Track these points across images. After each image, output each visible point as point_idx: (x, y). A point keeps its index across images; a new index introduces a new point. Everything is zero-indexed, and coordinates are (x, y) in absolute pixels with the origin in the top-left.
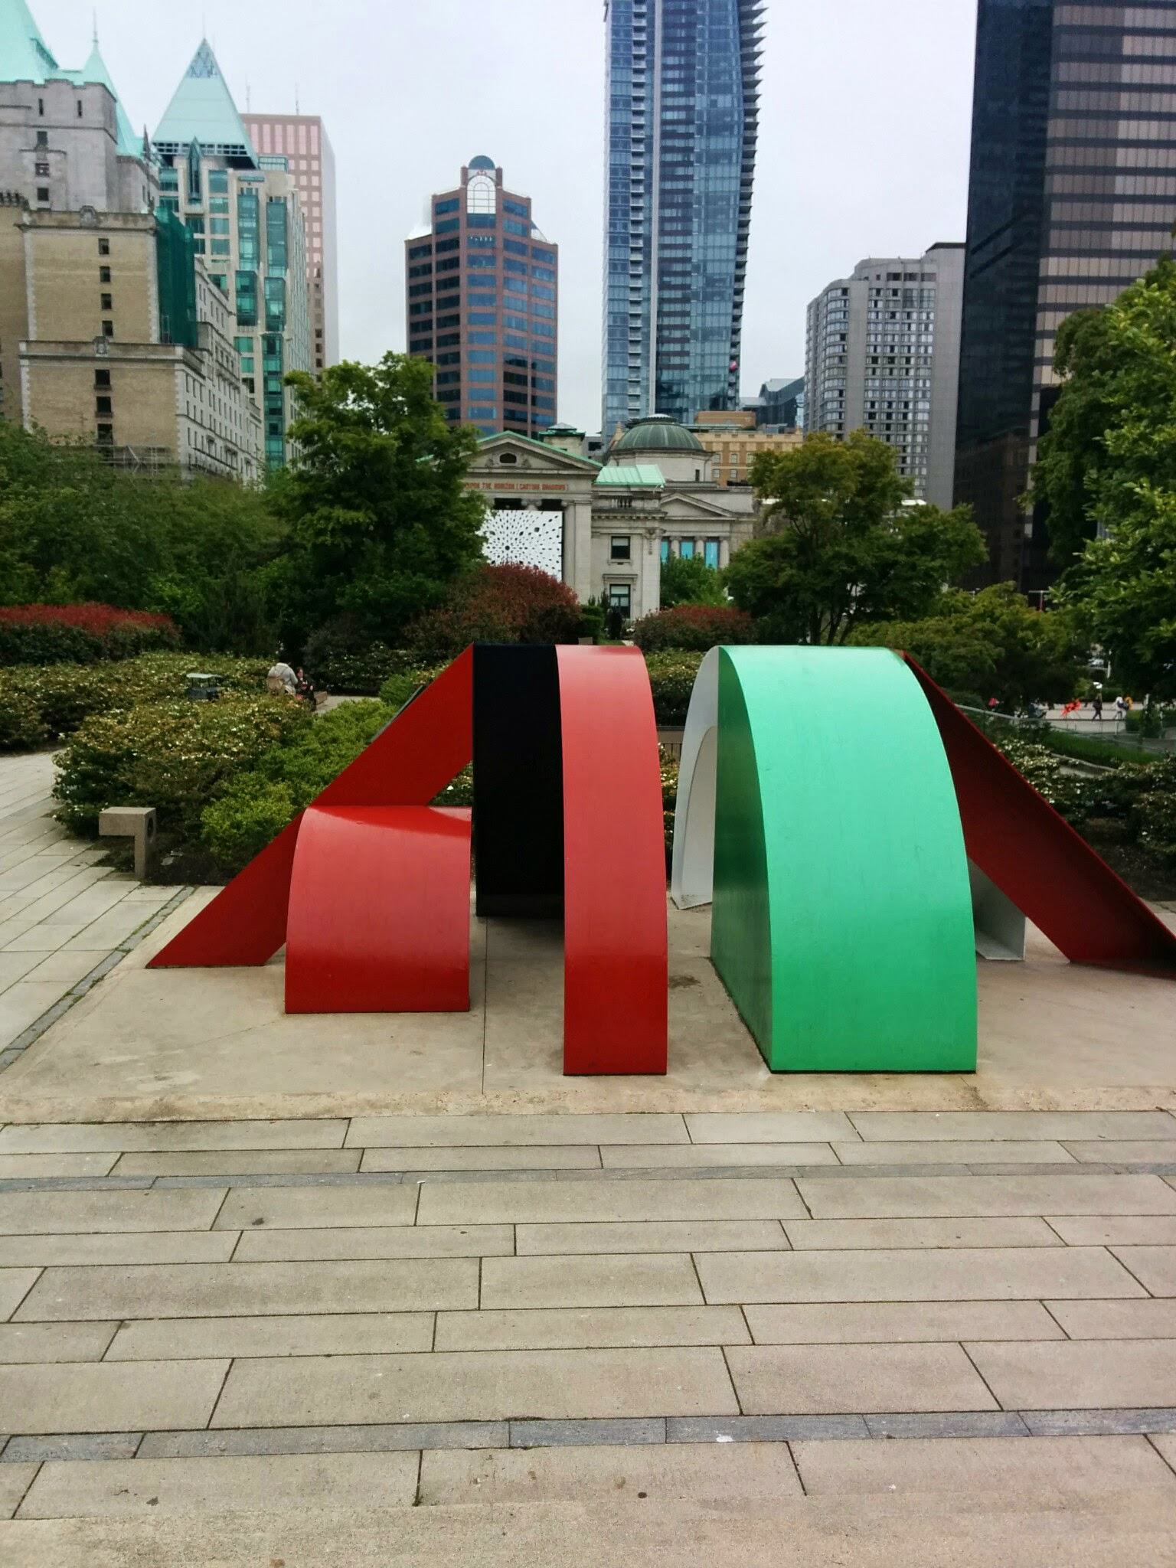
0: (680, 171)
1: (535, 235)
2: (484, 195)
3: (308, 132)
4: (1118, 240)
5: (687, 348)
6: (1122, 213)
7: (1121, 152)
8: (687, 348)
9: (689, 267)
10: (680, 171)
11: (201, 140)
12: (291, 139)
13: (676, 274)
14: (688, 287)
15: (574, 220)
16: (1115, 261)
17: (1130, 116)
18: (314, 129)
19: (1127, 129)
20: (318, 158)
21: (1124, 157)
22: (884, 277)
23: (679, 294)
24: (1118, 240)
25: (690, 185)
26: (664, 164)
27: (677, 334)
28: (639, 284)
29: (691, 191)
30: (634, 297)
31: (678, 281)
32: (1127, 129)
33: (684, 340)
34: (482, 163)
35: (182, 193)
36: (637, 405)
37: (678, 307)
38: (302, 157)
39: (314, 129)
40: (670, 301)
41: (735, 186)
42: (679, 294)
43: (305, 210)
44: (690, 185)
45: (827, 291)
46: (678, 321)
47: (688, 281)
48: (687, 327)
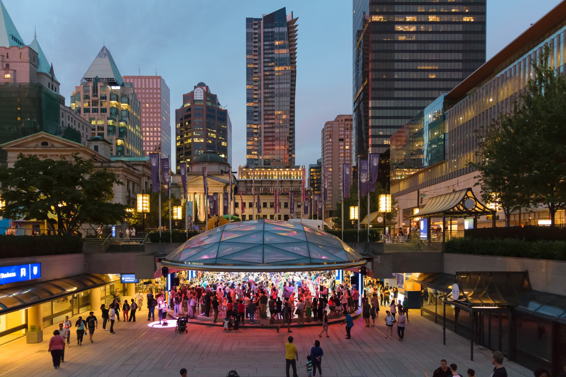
0: (270, 86)
1: (220, 107)
2: (200, 94)
3: (157, 81)
4: (396, 94)
5: (274, 143)
6: (397, 85)
7: (396, 64)
8: (274, 143)
9: (274, 117)
10: (270, 86)
11: (99, 77)
12: (151, 83)
16: (396, 101)
17: (398, 51)
18: (159, 80)
19: (397, 56)
20: (160, 89)
21: (397, 66)
22: (344, 120)
23: (271, 126)
24: (396, 94)
25: (274, 90)
26: (265, 84)
27: (271, 139)
29: (274, 92)
32: (397, 56)
33: (273, 141)
34: (201, 85)
35: (91, 94)
37: (271, 130)
39: (159, 80)
41: (289, 91)
42: (271, 126)
43: (140, 100)
44: (274, 90)
45: (326, 125)
46: (271, 134)
48: (274, 136)
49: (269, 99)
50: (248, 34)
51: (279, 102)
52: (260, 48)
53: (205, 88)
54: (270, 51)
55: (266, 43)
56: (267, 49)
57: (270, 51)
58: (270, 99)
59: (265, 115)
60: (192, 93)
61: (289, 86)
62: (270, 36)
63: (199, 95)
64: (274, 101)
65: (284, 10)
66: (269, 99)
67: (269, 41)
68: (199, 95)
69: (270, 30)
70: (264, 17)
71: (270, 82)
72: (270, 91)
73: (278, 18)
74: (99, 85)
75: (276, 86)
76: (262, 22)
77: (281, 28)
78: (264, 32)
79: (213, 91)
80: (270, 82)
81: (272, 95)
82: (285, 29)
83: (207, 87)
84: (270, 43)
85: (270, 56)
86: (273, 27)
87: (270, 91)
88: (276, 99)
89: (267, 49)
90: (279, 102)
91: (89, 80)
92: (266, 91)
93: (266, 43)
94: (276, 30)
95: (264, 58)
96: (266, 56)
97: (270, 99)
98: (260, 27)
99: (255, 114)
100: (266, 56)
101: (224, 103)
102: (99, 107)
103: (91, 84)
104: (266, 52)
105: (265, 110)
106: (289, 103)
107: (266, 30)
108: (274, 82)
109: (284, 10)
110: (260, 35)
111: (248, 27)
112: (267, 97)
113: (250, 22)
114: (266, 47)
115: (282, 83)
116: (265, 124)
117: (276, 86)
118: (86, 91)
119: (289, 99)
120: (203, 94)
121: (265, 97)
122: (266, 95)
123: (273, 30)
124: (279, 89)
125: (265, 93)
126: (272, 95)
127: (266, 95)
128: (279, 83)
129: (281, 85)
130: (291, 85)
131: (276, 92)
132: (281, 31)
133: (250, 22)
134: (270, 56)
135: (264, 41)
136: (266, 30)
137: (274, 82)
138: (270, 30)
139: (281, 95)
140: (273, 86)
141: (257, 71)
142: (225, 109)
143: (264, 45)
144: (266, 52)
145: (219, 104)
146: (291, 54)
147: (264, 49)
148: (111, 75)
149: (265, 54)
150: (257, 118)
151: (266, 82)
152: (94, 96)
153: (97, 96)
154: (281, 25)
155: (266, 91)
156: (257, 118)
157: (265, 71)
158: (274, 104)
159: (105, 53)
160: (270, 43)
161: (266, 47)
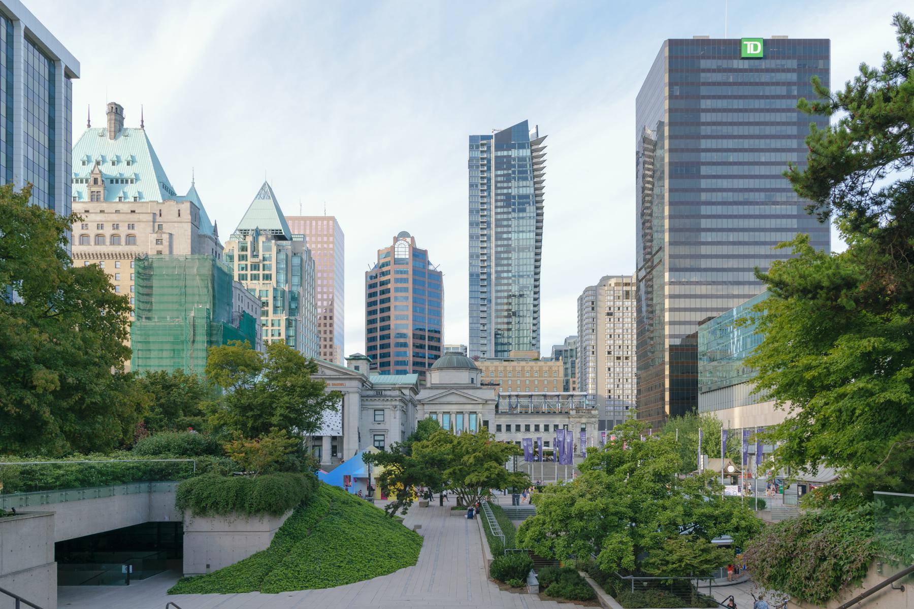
0: (505, 236)
10: (505, 236)
13: (505, 285)
14: (510, 291)
15: (452, 260)
25: (510, 242)
26: (496, 233)
28: (485, 289)
30: (483, 296)
31: (505, 288)
34: (404, 235)
36: (485, 349)
38: (319, 235)
40: (500, 298)
41: (533, 242)
44: (510, 242)
47: (510, 288)
49: (502, 256)
50: (471, 160)
51: (519, 259)
52: (489, 179)
53: (409, 240)
54: (505, 185)
55: (499, 173)
56: (500, 182)
57: (505, 185)
58: (505, 255)
59: (496, 278)
60: (393, 248)
61: (533, 235)
63: (403, 252)
64: (510, 265)
65: (525, 123)
66: (502, 256)
67: (504, 169)
68: (403, 252)
69: (505, 153)
70: (496, 135)
71: (505, 229)
72: (505, 243)
73: (515, 135)
75: (513, 236)
76: (493, 141)
77: (521, 151)
78: (496, 157)
79: (420, 246)
80: (505, 229)
81: (508, 249)
82: (526, 153)
83: (413, 239)
84: (506, 172)
85: (505, 191)
86: (509, 149)
87: (505, 243)
88: (514, 255)
89: (500, 182)
90: (519, 259)
91: (245, 233)
92: (499, 243)
93: (499, 173)
94: (514, 153)
95: (496, 195)
96: (499, 191)
97: (505, 255)
98: (489, 148)
99: (485, 277)
100: (499, 191)
101: (436, 261)
102: (261, 272)
103: (249, 239)
104: (499, 185)
105: (496, 272)
106: (533, 261)
107: (499, 154)
108: (510, 229)
109: (525, 123)
110: (489, 161)
111: (471, 147)
112: (501, 252)
113: (476, 142)
114: (499, 179)
115: (523, 232)
116: (497, 291)
117: (513, 236)
118: (244, 249)
119: (532, 255)
120: (407, 250)
121: (496, 252)
122: (499, 249)
123: (510, 153)
124: (518, 240)
125: (497, 246)
126: (508, 249)
127: (499, 249)
128: (519, 232)
129: (521, 234)
130: (537, 235)
131: (514, 244)
132: (521, 154)
133: (476, 142)
134: (505, 191)
135: (497, 169)
136: (499, 154)
137: (510, 229)
138: (505, 153)
139: (521, 249)
140: (510, 236)
141: (485, 213)
142: (438, 270)
143: (496, 176)
144: (499, 185)
145: (429, 263)
146: (536, 189)
147: (497, 182)
148: (278, 226)
149: (497, 188)
150: (485, 283)
151: (499, 230)
152: (254, 256)
153: (257, 256)
154: (522, 146)
155: (499, 243)
156: (485, 283)
157: (496, 213)
158: (510, 262)
159: (266, 192)
160: (506, 172)
161: (499, 179)
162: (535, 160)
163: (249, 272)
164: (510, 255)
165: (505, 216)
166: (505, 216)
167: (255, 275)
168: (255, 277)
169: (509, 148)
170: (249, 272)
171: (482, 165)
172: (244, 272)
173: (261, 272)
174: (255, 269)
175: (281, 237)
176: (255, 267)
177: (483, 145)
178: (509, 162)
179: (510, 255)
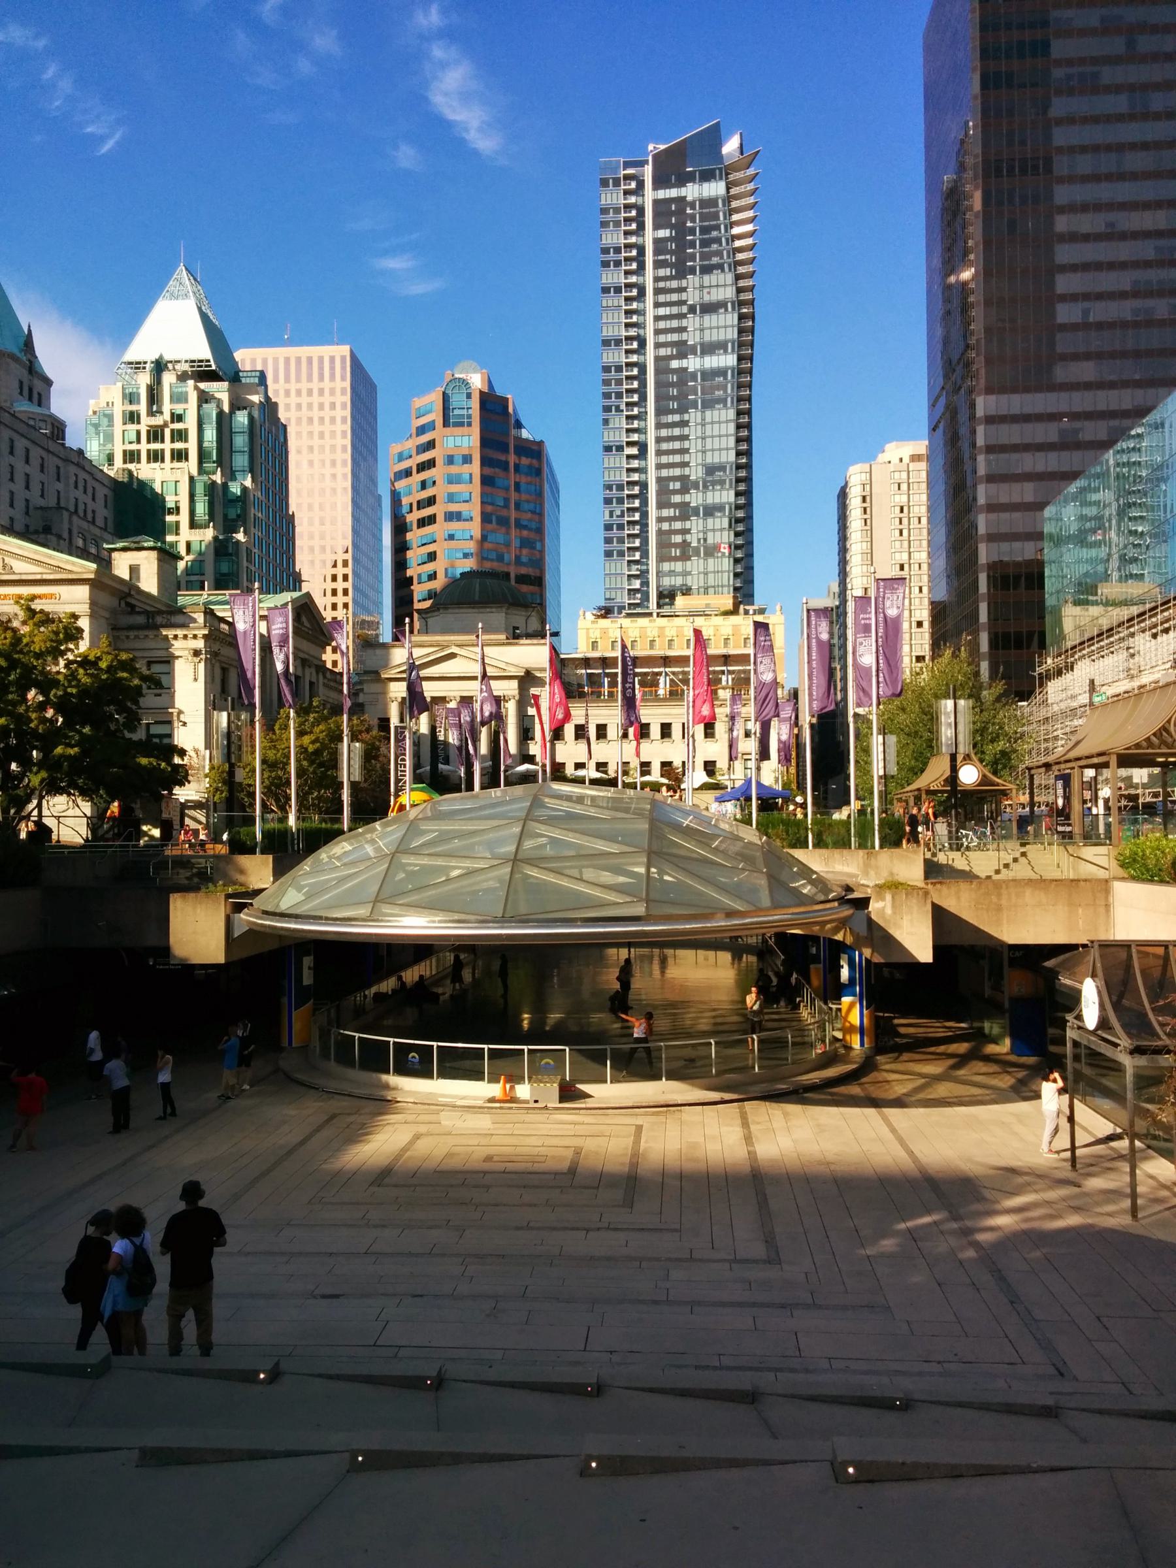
11: (167, 357)
35: (142, 407)
62: (672, 213)
69: (673, 193)
74: (168, 379)
76: (648, 171)
77: (706, 185)
78: (656, 202)
94: (691, 191)
98: (641, 184)
102: (167, 446)
107: (662, 194)
110: (641, 210)
118: (132, 398)
136: (662, 194)
138: (673, 193)
152: (151, 413)
162: (734, 204)
163: (144, 447)
164: (686, 417)
165: (675, 324)
166: (675, 324)
167: (156, 452)
168: (156, 457)
169: (682, 181)
170: (144, 447)
171: (627, 220)
172: (134, 447)
173: (167, 446)
174: (156, 440)
175: (211, 376)
176: (155, 434)
177: (628, 178)
178: (681, 212)
179: (686, 417)
